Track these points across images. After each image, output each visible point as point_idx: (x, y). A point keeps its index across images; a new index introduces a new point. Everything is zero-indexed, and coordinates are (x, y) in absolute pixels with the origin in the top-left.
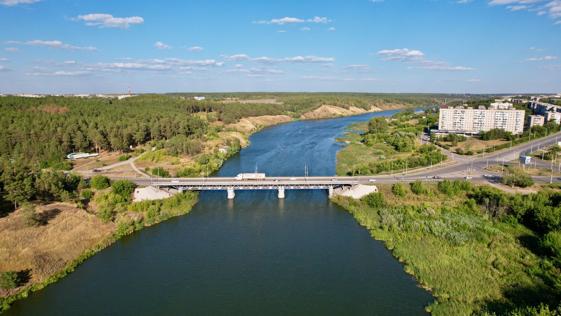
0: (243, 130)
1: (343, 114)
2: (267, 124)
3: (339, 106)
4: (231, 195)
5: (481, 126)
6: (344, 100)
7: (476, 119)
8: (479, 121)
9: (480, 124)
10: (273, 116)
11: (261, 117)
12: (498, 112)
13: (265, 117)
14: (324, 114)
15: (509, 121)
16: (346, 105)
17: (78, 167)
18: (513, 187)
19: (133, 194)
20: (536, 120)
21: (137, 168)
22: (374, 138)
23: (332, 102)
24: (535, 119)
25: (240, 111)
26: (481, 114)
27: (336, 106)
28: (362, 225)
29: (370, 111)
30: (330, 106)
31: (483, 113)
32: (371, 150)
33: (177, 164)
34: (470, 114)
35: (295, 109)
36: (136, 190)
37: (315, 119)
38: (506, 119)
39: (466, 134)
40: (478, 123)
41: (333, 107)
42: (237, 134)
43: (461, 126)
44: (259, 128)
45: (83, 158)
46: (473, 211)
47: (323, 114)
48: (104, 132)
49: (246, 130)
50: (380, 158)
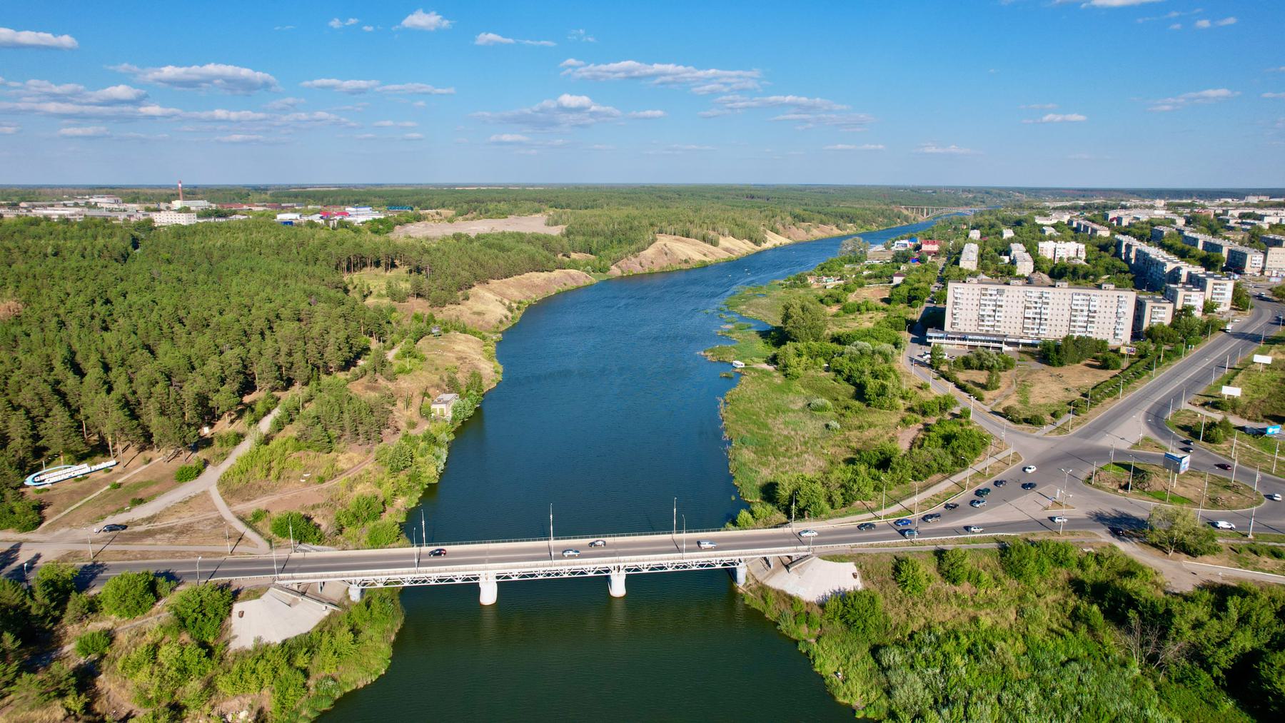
0: (481, 323)
1: (707, 259)
2: (534, 296)
5: (1040, 324)
6: (707, 221)
7: (1029, 308)
8: (1036, 313)
9: (1038, 321)
10: (545, 275)
12: (1079, 295)
13: (528, 279)
14: (663, 263)
15: (1102, 315)
16: (712, 234)
17: (60, 512)
18: (1170, 554)
19: (228, 621)
20: (1156, 310)
21: (229, 505)
23: (679, 227)
24: (1154, 307)
26: (1040, 298)
27: (688, 236)
28: (840, 700)
29: (765, 246)
30: (674, 237)
31: (1045, 295)
33: (332, 479)
34: (1016, 297)
35: (595, 246)
36: (237, 607)
37: (642, 275)
38: (1095, 312)
39: (1008, 344)
40: (1035, 318)
42: (467, 340)
43: (997, 324)
44: (517, 312)
45: (71, 478)
46: (1101, 643)
47: (661, 261)
48: (130, 398)
49: (488, 323)
50: (827, 426)
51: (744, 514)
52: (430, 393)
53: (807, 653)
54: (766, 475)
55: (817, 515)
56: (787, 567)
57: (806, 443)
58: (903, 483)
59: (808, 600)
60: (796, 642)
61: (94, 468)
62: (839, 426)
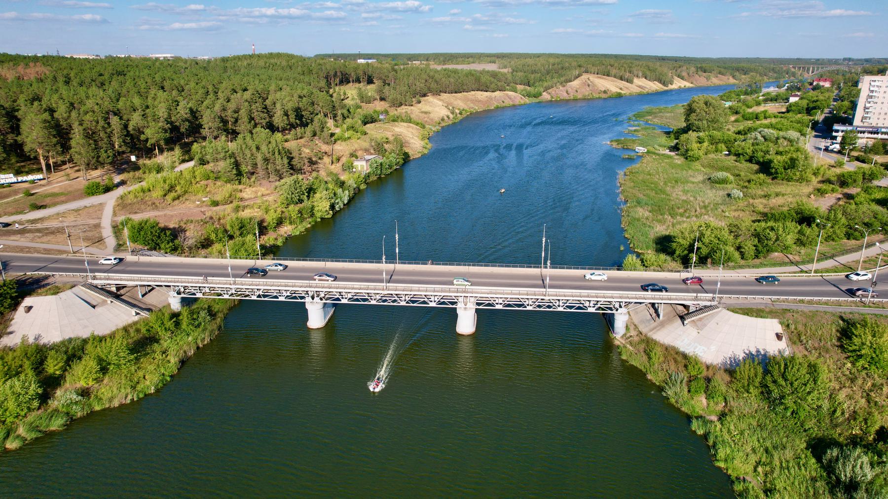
0: (426, 119)
1: (623, 92)
2: (477, 108)
3: (615, 77)
4: (316, 319)
6: (625, 65)
11: (465, 93)
13: (473, 95)
14: (586, 92)
16: (627, 75)
22: (700, 143)
25: (423, 81)
27: (608, 75)
29: (671, 87)
30: (597, 76)
32: (697, 174)
37: (567, 101)
41: (605, 79)
42: (409, 127)
44: (459, 115)
47: (584, 90)
49: (432, 120)
50: (729, 195)
51: (631, 259)
52: (358, 155)
53: (706, 436)
54: (661, 230)
55: (727, 262)
56: (682, 318)
57: (705, 207)
58: (833, 240)
59: (709, 362)
60: (689, 418)
61: (20, 179)
62: (742, 195)
